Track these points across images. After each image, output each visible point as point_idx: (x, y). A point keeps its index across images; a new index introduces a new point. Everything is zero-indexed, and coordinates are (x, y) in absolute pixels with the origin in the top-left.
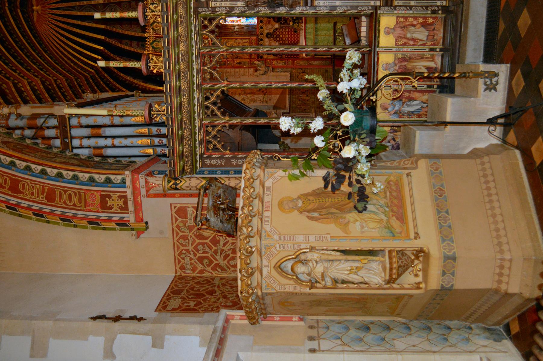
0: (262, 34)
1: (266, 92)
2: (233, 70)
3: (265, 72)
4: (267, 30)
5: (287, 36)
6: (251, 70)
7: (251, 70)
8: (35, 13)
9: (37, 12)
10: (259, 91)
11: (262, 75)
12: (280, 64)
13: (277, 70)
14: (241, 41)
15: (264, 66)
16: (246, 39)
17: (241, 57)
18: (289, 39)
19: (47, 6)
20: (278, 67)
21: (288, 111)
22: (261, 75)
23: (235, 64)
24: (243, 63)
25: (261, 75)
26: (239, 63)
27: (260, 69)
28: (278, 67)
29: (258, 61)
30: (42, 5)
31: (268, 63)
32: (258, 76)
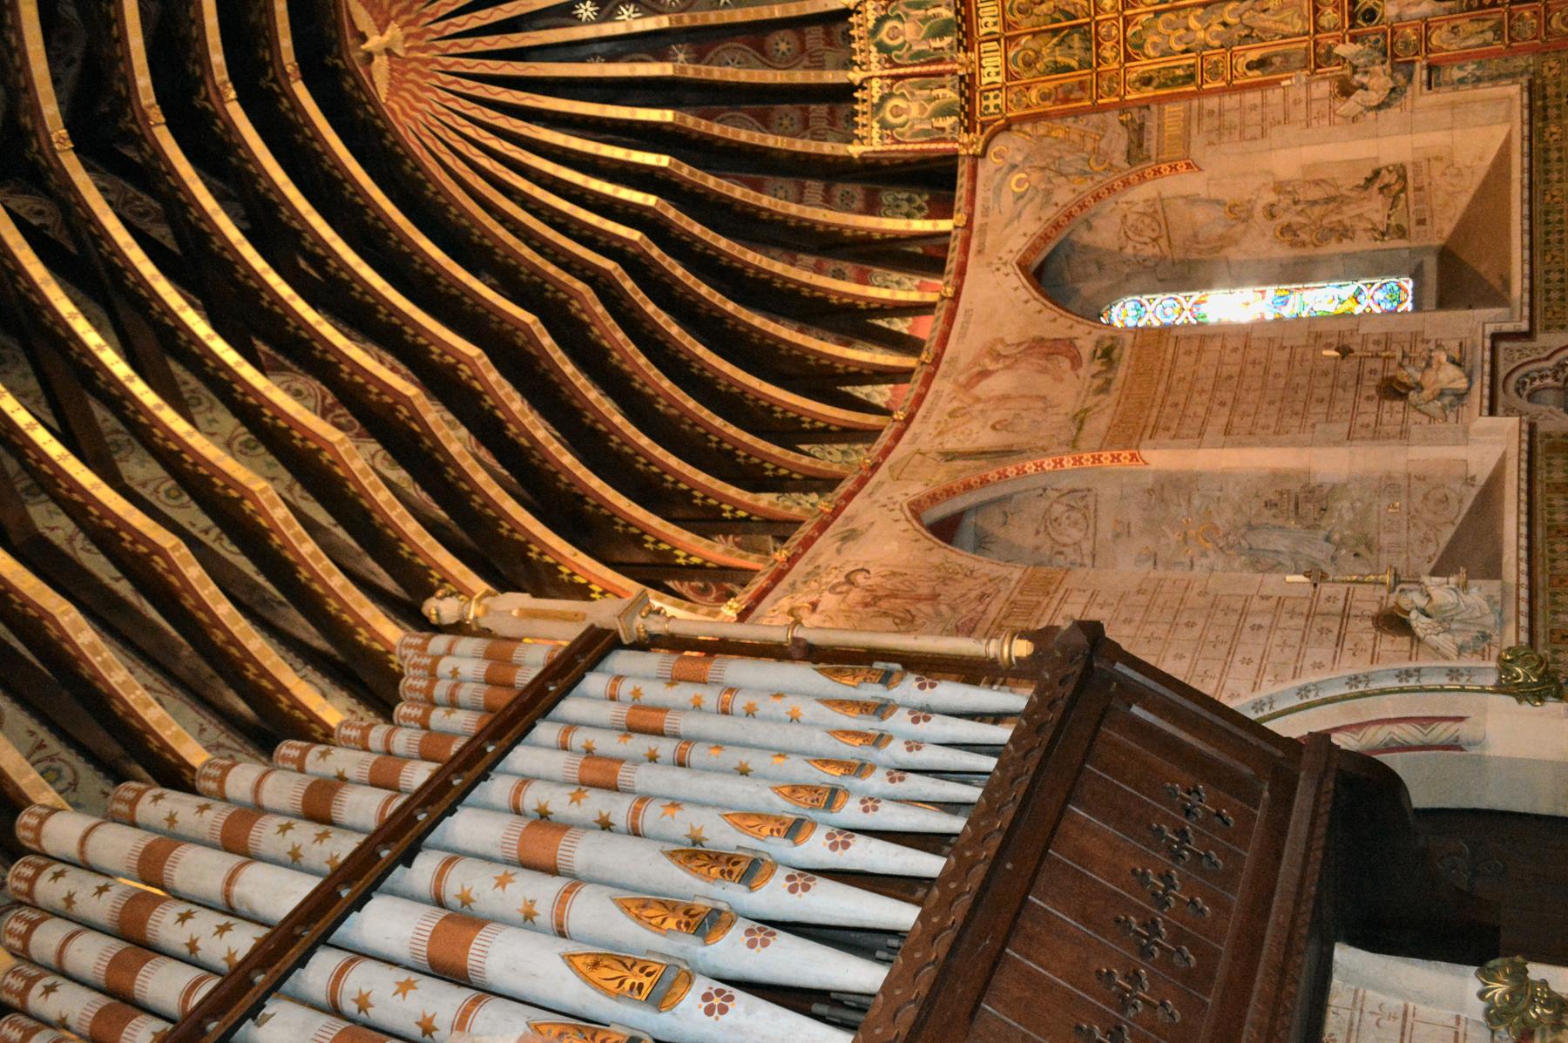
1: (1404, 189)
2: (1231, 101)
3: (1393, 90)
7: (1323, 89)
8: (381, 65)
9: (389, 52)
10: (1365, 187)
11: (1379, 107)
13: (1457, 74)
15: (1387, 66)
17: (1264, 30)
19: (426, 15)
20: (1461, 59)
21: (1524, 326)
22: (1369, 109)
23: (1241, 68)
24: (1277, 61)
25: (1369, 109)
26: (1262, 64)
27: (1365, 80)
28: (1461, 59)
29: (1354, 39)
30: (404, 18)
31: (1407, 44)
32: (1354, 119)
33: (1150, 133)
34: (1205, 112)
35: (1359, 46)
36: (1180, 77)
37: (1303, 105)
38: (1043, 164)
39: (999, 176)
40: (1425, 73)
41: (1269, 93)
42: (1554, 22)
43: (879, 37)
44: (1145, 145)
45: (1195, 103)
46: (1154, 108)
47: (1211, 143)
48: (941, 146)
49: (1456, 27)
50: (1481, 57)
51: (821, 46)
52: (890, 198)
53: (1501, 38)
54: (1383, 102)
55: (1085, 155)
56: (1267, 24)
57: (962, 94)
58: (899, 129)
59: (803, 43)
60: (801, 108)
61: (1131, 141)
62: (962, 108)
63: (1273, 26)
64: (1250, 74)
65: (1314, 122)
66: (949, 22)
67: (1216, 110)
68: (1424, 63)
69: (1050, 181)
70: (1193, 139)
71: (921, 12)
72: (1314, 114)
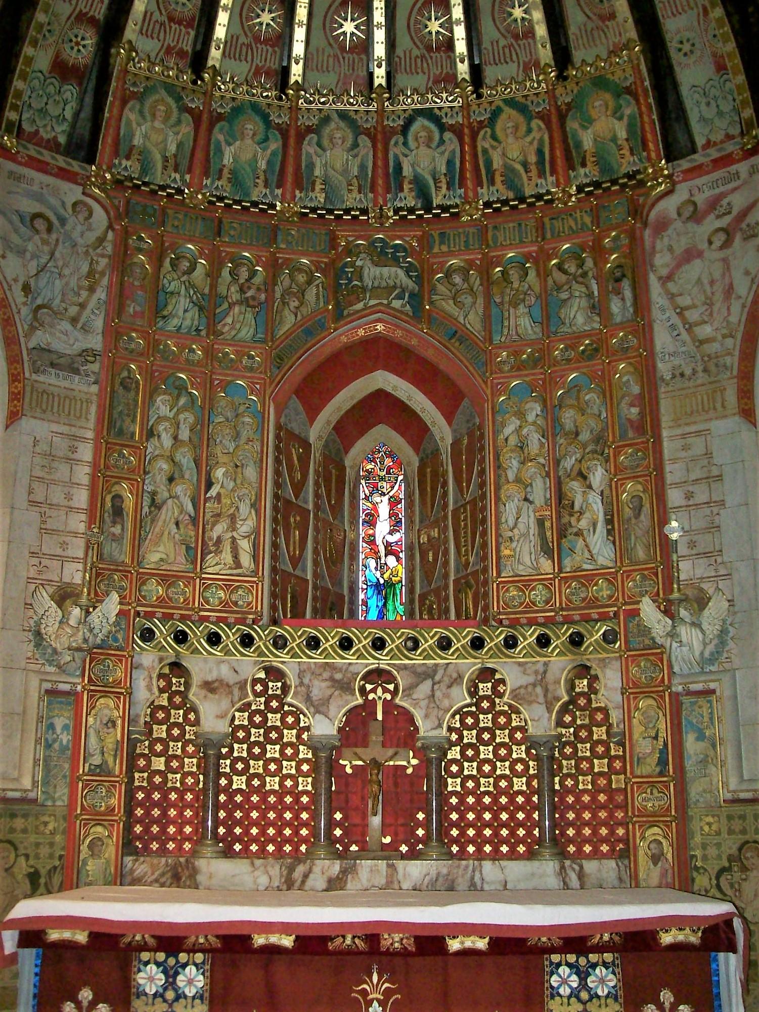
0: (279, 643)
2: (83, 474)
3: (55, 651)
4: (301, 675)
5: (273, 783)
6: (75, 574)
7: (75, 574)
11: (38, 634)
12: (93, 740)
14: (245, 528)
16: (255, 557)
18: (255, 799)
22: (38, 624)
24: (117, 530)
26: (118, 512)
29: (121, 613)
33: (65, 379)
34: (76, 444)
35: (113, 619)
36: (123, 421)
37: (59, 551)
38: (57, 254)
39: (53, 201)
40: (66, 687)
41: (83, 517)
42: (99, 829)
43: (250, 111)
44: (53, 371)
45: (90, 435)
46: (95, 389)
47: (36, 442)
48: (108, 150)
49: (114, 724)
50: (75, 750)
51: (257, 61)
52: (68, 94)
53: (91, 773)
54: (42, 639)
55: (57, 301)
56: (160, 523)
57: (163, 188)
58: (138, 107)
59: (266, 42)
60: (193, 19)
61: (61, 356)
62: (145, 184)
63: (157, 530)
64: (108, 498)
65: (35, 561)
66: (248, 194)
67: (75, 456)
68: (79, 688)
69: (34, 256)
70: (46, 424)
71: (262, 165)
72: (45, 562)
